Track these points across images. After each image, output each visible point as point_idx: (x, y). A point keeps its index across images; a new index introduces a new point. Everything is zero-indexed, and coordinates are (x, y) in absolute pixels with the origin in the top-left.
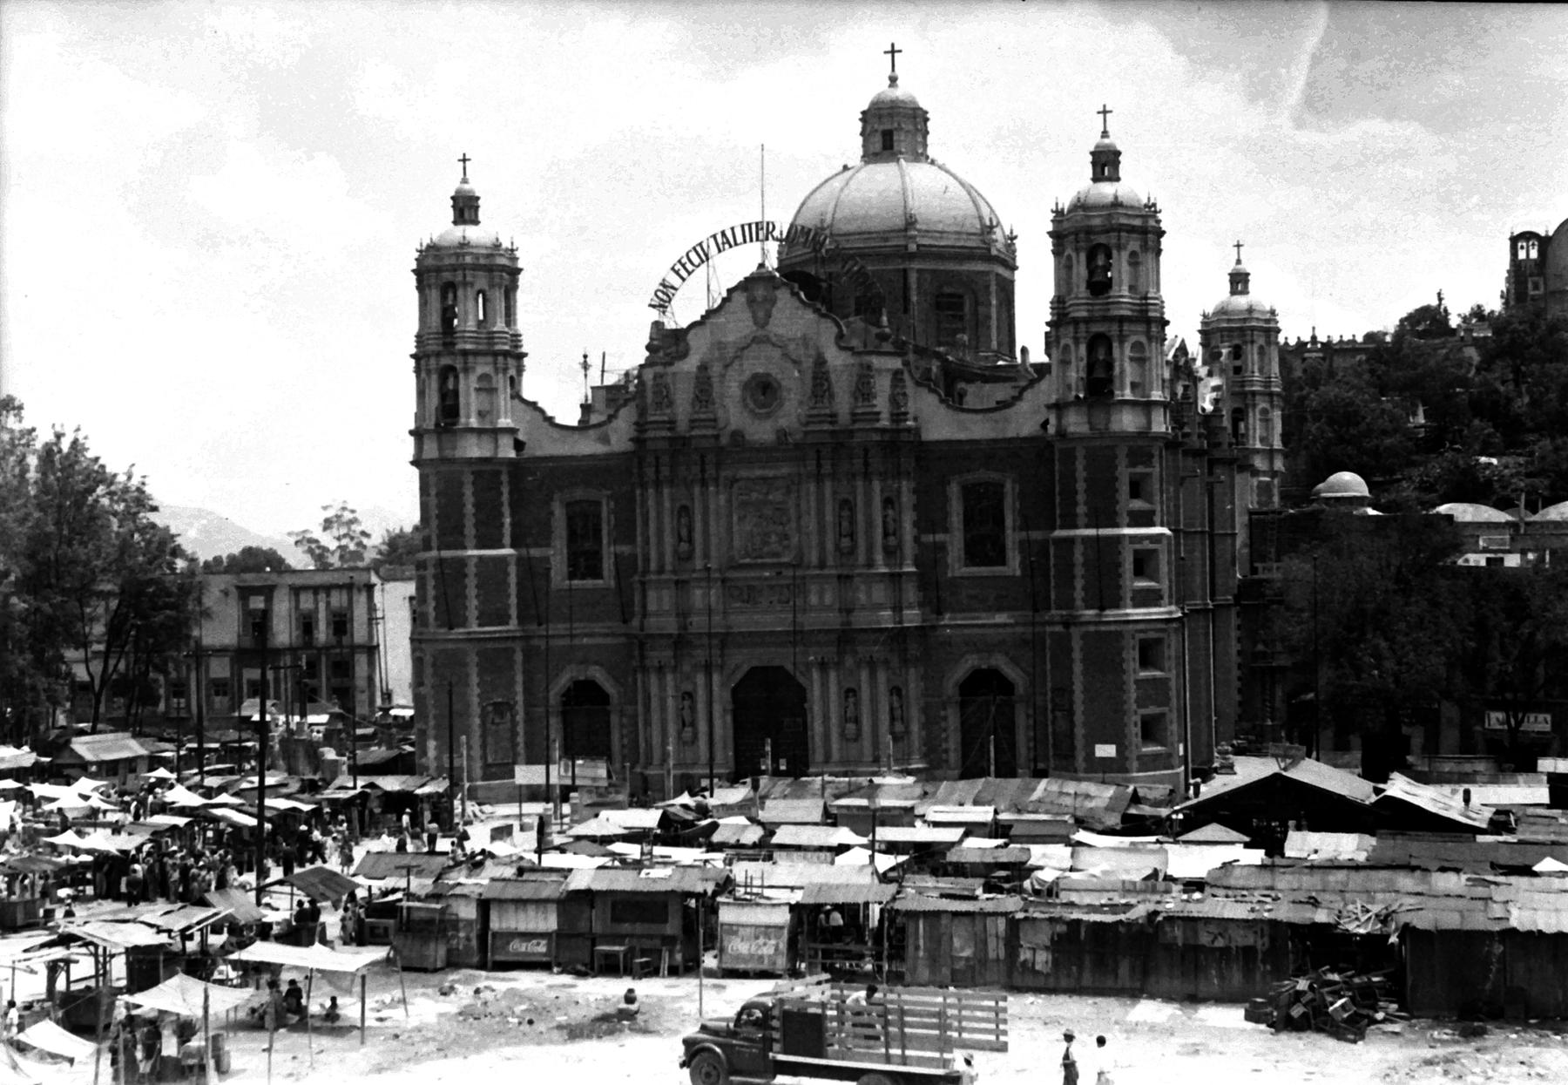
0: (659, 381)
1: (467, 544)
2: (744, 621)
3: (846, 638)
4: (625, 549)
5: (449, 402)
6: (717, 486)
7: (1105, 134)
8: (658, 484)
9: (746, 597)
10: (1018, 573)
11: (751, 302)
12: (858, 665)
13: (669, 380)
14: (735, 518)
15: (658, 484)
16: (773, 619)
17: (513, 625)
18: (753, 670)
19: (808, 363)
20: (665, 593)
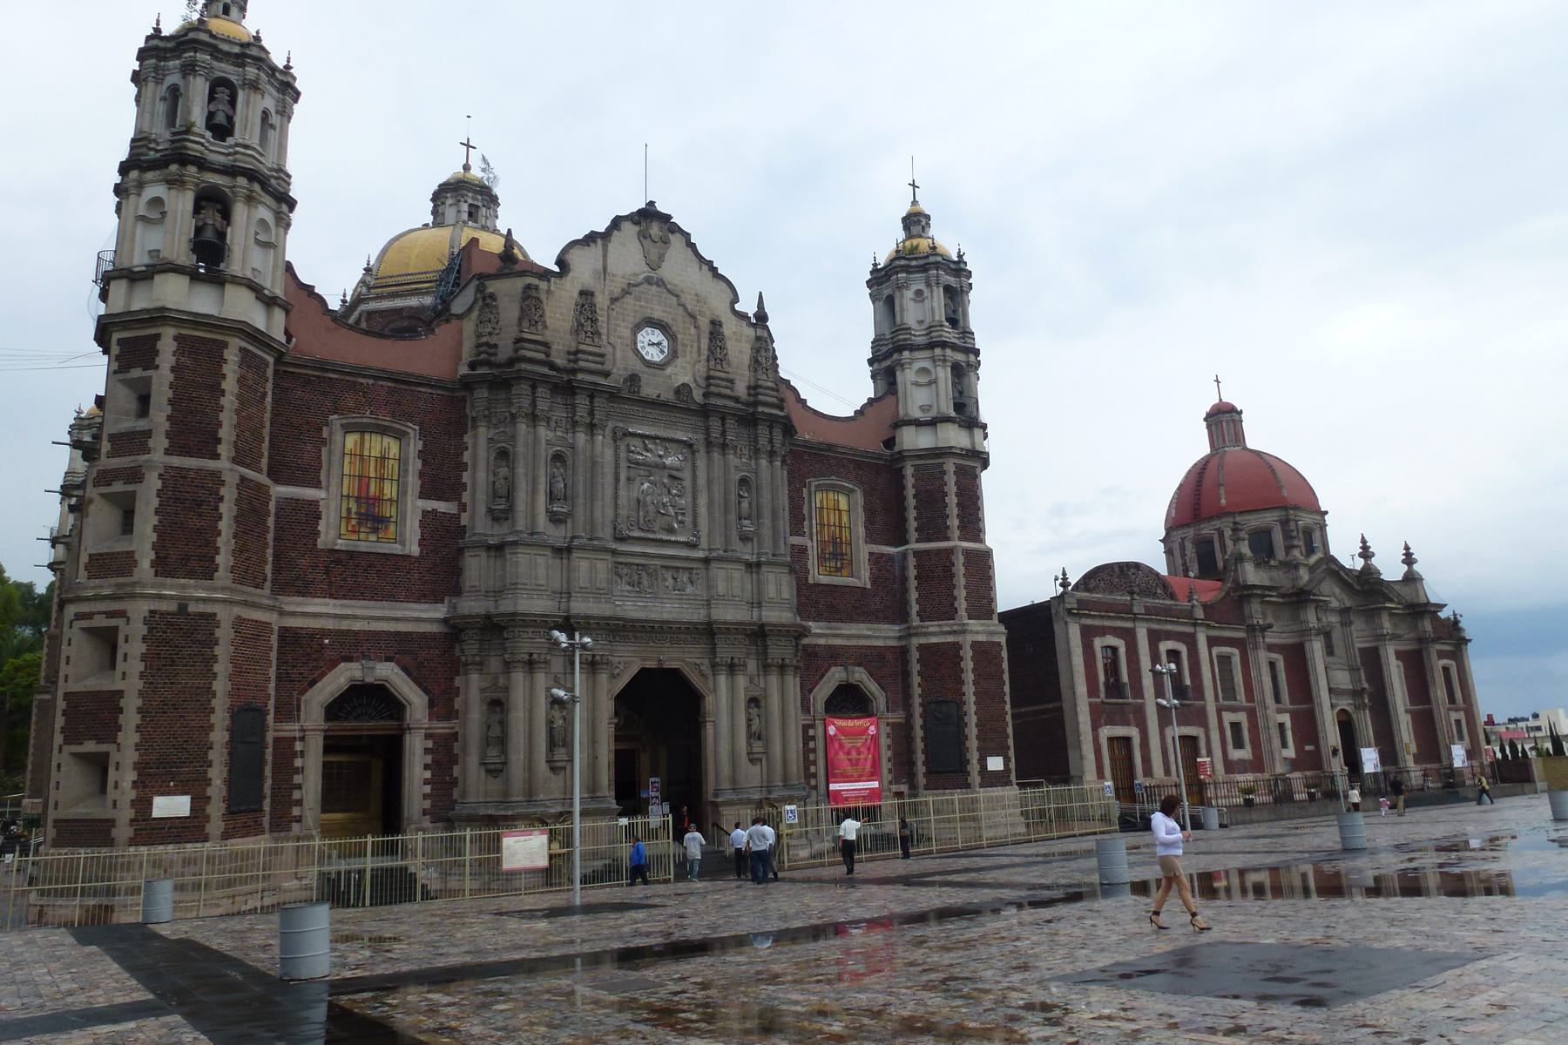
0: (534, 294)
1: (224, 450)
2: (632, 608)
3: (759, 634)
4: (442, 506)
5: (209, 235)
6: (604, 437)
7: (915, 202)
8: (534, 418)
9: (636, 578)
10: (869, 586)
11: (643, 236)
12: (765, 667)
13: (543, 297)
14: (623, 477)
15: (534, 418)
16: (668, 609)
17: (267, 591)
18: (643, 671)
19: (704, 323)
20: (541, 560)
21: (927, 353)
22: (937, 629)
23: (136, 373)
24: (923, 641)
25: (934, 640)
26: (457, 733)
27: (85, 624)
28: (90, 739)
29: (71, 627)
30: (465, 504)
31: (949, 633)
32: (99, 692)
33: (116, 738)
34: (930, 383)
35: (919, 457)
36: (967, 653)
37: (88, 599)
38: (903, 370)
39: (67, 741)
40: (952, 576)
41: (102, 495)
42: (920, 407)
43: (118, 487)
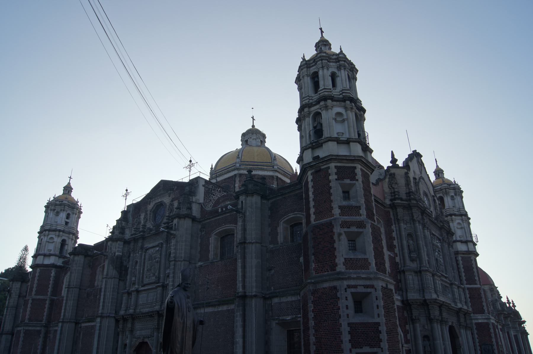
21: (460, 218)
22: (480, 317)
23: (348, 181)
24: (476, 321)
25: (480, 321)
26: (410, 349)
27: (353, 290)
28: (366, 346)
29: (346, 291)
30: (396, 254)
31: (485, 319)
32: (367, 323)
33: (380, 345)
34: (462, 228)
35: (463, 254)
36: (491, 326)
37: (354, 279)
38: (453, 222)
39: (354, 346)
40: (481, 298)
41: (345, 232)
42: (459, 236)
43: (353, 229)
